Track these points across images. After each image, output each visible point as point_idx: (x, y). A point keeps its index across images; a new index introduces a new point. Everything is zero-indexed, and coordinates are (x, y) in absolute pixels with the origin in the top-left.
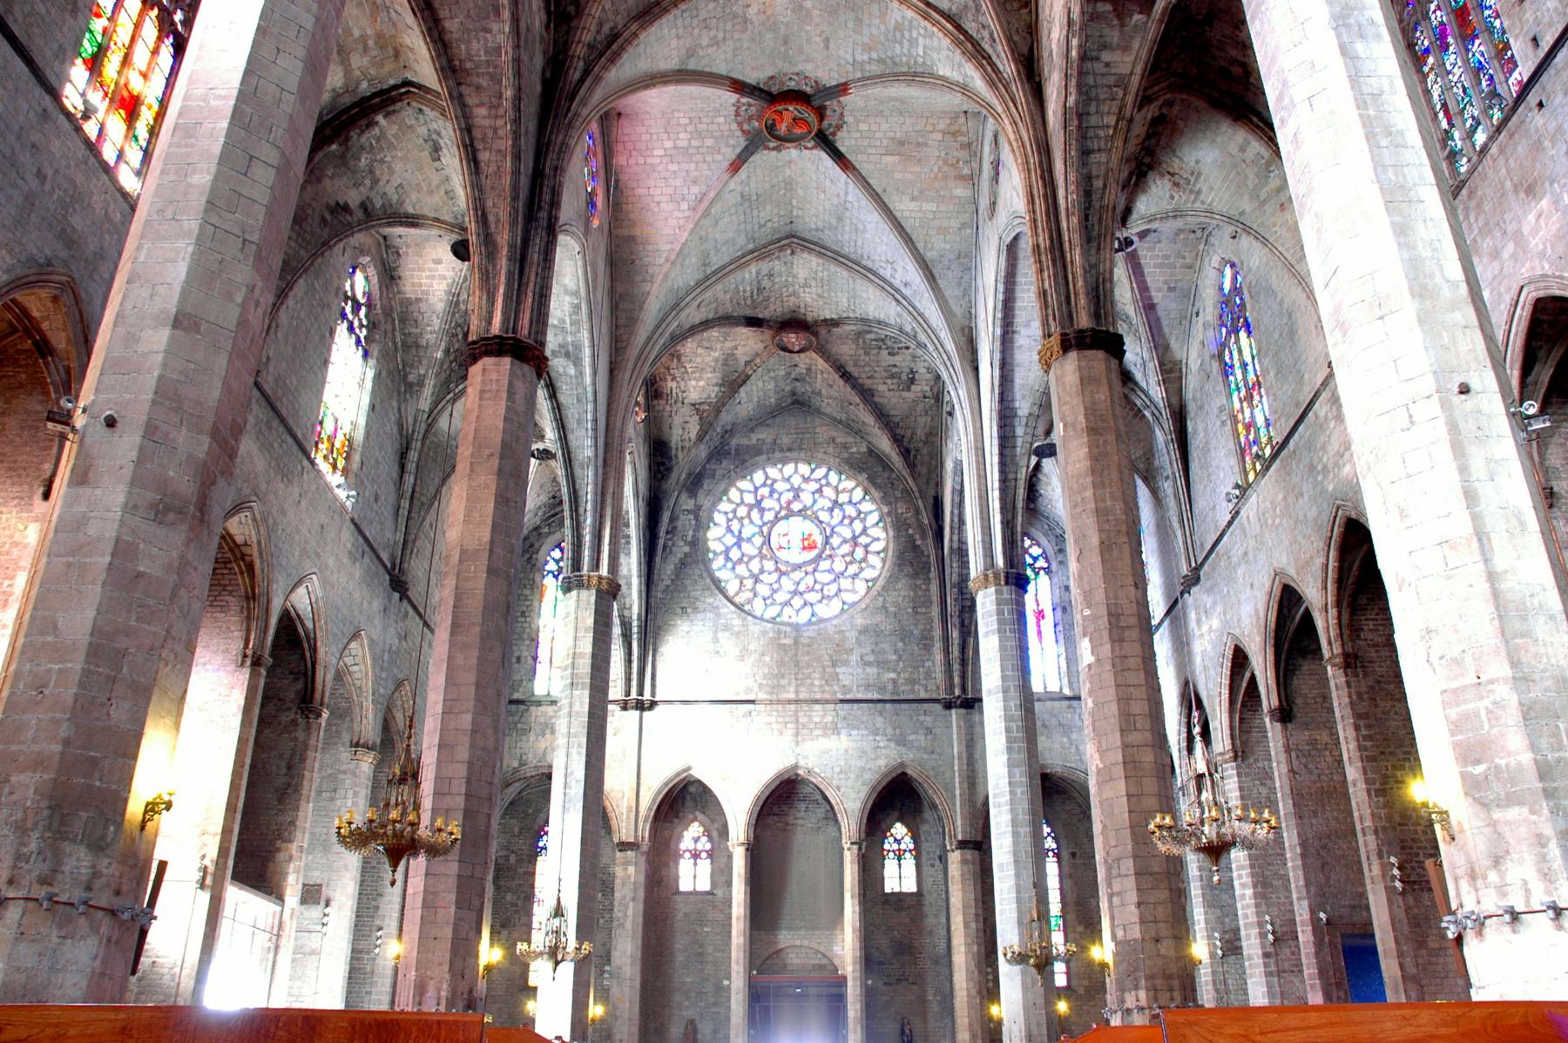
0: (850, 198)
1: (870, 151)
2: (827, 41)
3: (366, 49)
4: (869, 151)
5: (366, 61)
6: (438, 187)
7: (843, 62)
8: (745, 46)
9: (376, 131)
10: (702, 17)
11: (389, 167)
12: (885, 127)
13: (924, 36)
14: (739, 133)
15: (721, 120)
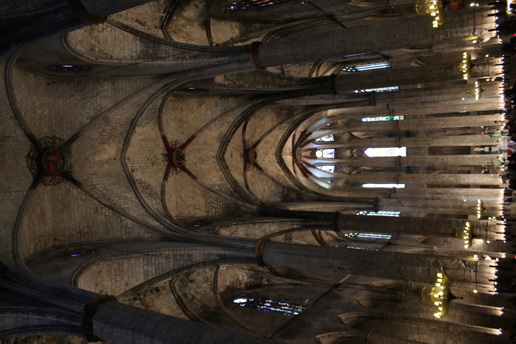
0: (13, 194)
1: (39, 199)
2: (96, 174)
3: (182, 26)
4: (39, 199)
5: (180, 23)
6: (126, 14)
7: (90, 181)
8: (92, 143)
9: (162, 11)
10: (118, 128)
11: (151, 7)
12: (47, 205)
13: (133, 206)
14: (40, 138)
15: (45, 130)
